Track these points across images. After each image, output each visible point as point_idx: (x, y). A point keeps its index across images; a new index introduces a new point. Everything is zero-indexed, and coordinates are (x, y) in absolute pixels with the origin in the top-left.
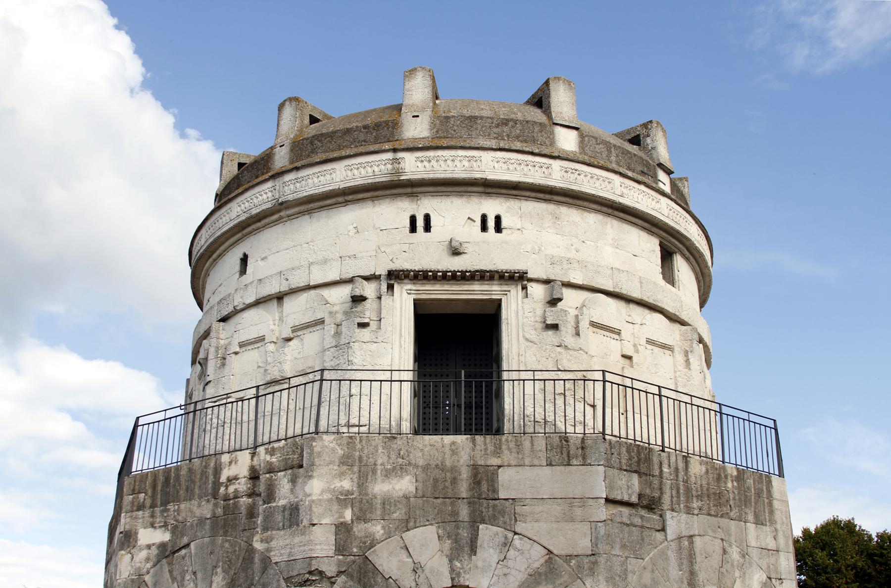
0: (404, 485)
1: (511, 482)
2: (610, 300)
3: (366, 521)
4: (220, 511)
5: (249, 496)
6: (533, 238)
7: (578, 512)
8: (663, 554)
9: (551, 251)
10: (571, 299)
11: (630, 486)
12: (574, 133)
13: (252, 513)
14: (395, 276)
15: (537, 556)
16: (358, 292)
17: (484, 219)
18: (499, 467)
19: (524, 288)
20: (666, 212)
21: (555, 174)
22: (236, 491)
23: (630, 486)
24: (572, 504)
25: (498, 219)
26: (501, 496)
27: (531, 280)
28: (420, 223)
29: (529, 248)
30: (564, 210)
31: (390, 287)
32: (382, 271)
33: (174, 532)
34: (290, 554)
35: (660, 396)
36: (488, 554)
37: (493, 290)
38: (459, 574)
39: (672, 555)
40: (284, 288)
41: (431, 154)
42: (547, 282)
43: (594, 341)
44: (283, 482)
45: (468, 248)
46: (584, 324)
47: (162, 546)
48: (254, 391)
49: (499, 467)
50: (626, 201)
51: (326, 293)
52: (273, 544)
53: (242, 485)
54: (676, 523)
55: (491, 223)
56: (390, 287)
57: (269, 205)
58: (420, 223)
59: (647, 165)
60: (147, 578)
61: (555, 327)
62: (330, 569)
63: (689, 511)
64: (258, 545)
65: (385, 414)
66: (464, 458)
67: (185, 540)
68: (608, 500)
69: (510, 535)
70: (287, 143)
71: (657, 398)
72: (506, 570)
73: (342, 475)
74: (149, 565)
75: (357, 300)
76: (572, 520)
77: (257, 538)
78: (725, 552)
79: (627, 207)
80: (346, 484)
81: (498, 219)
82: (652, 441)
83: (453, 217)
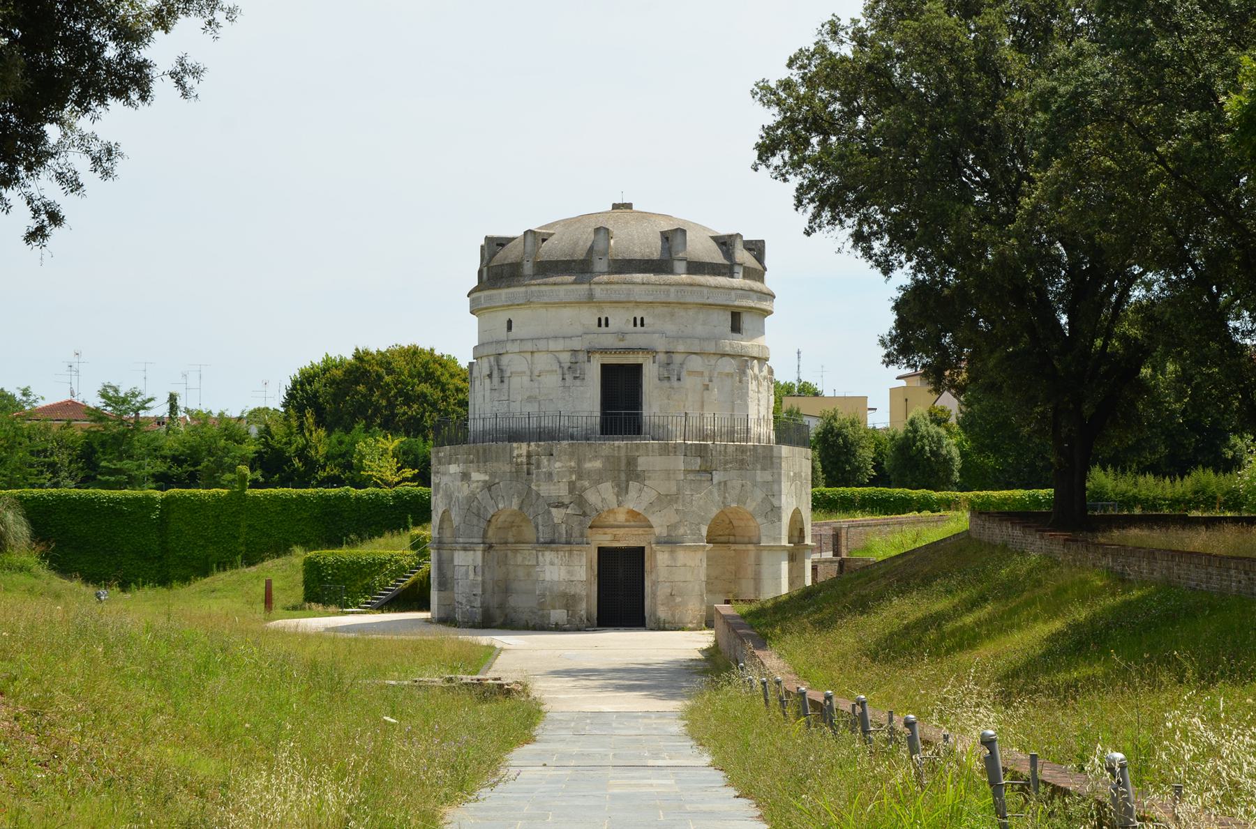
0: (598, 464)
1: (643, 463)
6: (661, 331)
8: (711, 493)
11: (697, 463)
13: (529, 473)
15: (654, 493)
24: (668, 474)
25: (642, 319)
28: (603, 322)
33: (491, 475)
36: (633, 493)
39: (715, 490)
44: (544, 460)
46: (684, 374)
47: (485, 482)
50: (710, 301)
53: (524, 459)
54: (717, 477)
55: (639, 322)
58: (603, 322)
62: (566, 501)
63: (725, 470)
64: (534, 487)
66: (623, 453)
80: (573, 464)
81: (642, 319)
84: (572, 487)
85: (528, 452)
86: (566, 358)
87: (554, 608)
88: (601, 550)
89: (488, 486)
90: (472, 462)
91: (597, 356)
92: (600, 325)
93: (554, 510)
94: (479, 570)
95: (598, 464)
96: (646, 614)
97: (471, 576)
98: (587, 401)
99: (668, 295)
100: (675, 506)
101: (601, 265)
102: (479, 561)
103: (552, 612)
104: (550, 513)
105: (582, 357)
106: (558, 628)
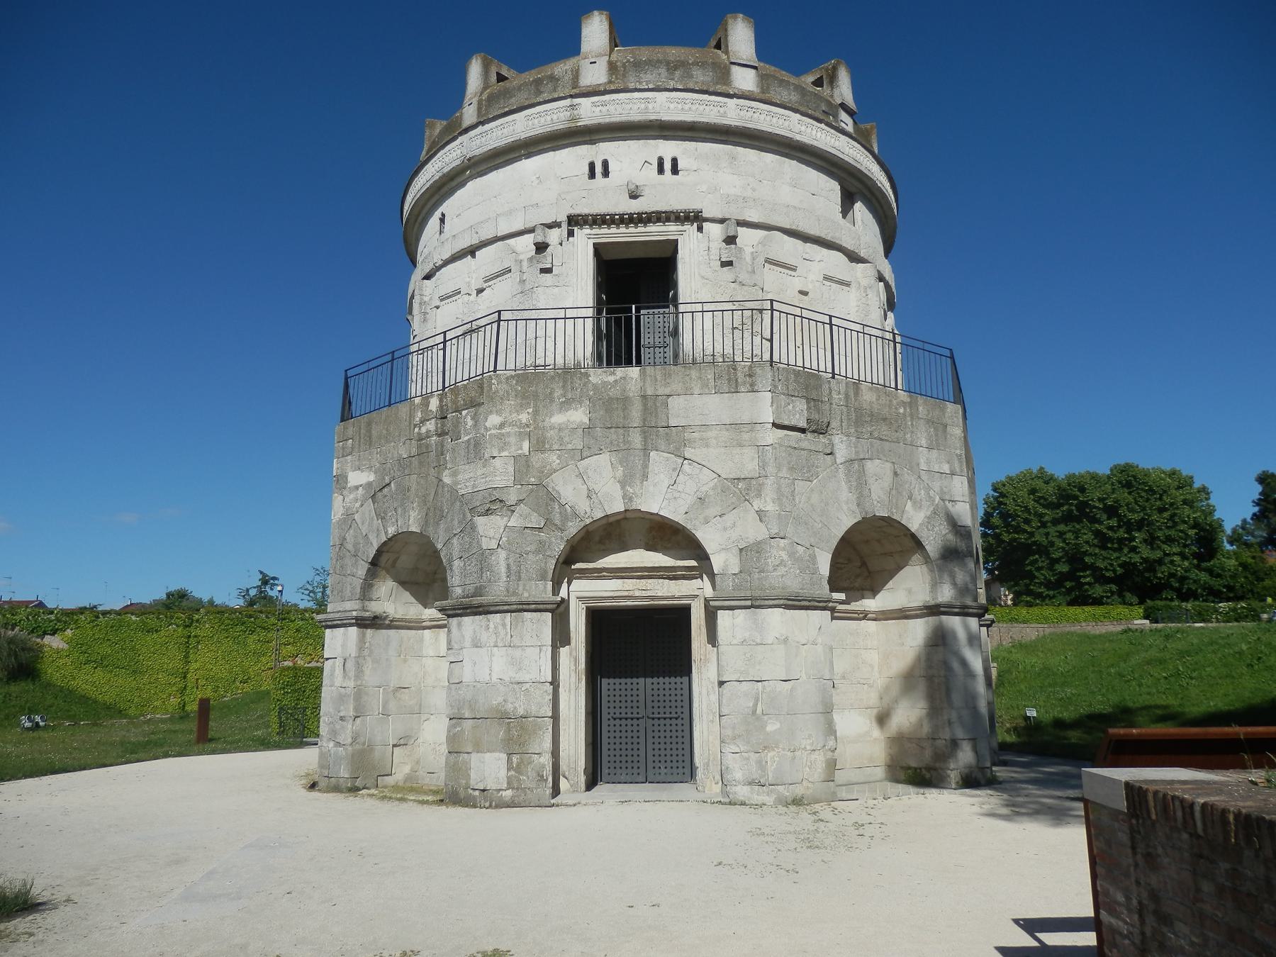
2: (786, 237)
3: (543, 451)
4: (414, 451)
5: (439, 435)
7: (746, 436)
10: (747, 237)
11: (798, 413)
12: (753, 71)
14: (575, 221)
16: (540, 239)
18: (669, 396)
19: (700, 229)
20: (847, 150)
21: (731, 113)
22: (428, 431)
23: (798, 413)
25: (675, 161)
26: (672, 423)
27: (707, 220)
28: (599, 169)
29: (704, 188)
31: (571, 234)
32: (563, 218)
34: (474, 486)
35: (831, 325)
37: (668, 230)
38: (631, 499)
40: (475, 241)
41: (607, 97)
42: (722, 221)
43: (773, 281)
45: (646, 192)
48: (440, 339)
49: (669, 396)
51: (512, 241)
52: (460, 477)
55: (668, 166)
56: (571, 234)
57: (458, 162)
58: (599, 169)
59: (829, 104)
60: (356, 517)
61: (730, 264)
62: (512, 498)
64: (447, 480)
65: (570, 355)
67: (387, 481)
68: (774, 425)
69: (680, 461)
70: (475, 101)
71: (827, 327)
72: (677, 495)
73: (522, 407)
74: (357, 505)
75: (541, 248)
76: (741, 446)
77: (446, 472)
78: (896, 474)
79: (805, 144)
80: (524, 417)
81: (675, 161)
82: (822, 368)
83: (630, 160)
84: (522, 464)
85: (441, 407)
86: (525, 244)
87: (478, 748)
88: (600, 619)
89: (375, 493)
91: (587, 230)
93: (480, 521)
94: (350, 665)
95: (578, 416)
96: (698, 761)
99: (724, 115)
100: (757, 504)
101: (594, 74)
102: (352, 650)
103: (474, 756)
104: (473, 528)
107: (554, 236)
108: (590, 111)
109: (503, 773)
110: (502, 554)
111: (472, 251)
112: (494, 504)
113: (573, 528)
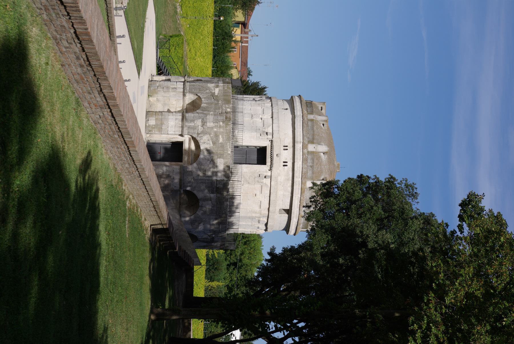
0: (221, 140)
6: (281, 174)
9: (279, 178)
17: (286, 162)
21: (298, 179)
25: (286, 165)
28: (286, 148)
30: (291, 182)
33: (217, 96)
55: (285, 164)
64: (211, 113)
70: (314, 118)
81: (286, 165)
83: (287, 155)
87: (156, 119)
89: (213, 95)
90: (224, 88)
91: (270, 144)
92: (284, 146)
93: (201, 120)
97: (171, 87)
98: (249, 139)
104: (199, 119)
105: (270, 137)
106: (147, 120)
107: (270, 137)
108: (299, 146)
109: (151, 124)
110: (193, 124)
111: (272, 117)
112: (204, 123)
113: (198, 139)
